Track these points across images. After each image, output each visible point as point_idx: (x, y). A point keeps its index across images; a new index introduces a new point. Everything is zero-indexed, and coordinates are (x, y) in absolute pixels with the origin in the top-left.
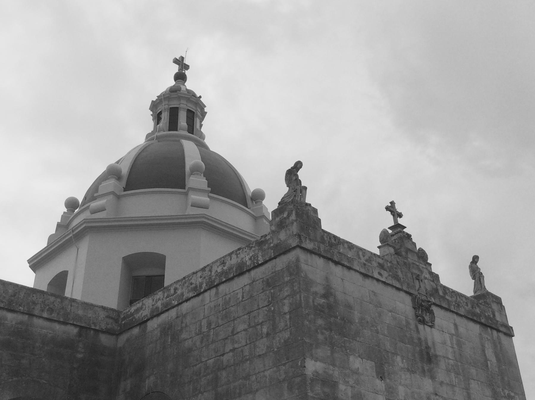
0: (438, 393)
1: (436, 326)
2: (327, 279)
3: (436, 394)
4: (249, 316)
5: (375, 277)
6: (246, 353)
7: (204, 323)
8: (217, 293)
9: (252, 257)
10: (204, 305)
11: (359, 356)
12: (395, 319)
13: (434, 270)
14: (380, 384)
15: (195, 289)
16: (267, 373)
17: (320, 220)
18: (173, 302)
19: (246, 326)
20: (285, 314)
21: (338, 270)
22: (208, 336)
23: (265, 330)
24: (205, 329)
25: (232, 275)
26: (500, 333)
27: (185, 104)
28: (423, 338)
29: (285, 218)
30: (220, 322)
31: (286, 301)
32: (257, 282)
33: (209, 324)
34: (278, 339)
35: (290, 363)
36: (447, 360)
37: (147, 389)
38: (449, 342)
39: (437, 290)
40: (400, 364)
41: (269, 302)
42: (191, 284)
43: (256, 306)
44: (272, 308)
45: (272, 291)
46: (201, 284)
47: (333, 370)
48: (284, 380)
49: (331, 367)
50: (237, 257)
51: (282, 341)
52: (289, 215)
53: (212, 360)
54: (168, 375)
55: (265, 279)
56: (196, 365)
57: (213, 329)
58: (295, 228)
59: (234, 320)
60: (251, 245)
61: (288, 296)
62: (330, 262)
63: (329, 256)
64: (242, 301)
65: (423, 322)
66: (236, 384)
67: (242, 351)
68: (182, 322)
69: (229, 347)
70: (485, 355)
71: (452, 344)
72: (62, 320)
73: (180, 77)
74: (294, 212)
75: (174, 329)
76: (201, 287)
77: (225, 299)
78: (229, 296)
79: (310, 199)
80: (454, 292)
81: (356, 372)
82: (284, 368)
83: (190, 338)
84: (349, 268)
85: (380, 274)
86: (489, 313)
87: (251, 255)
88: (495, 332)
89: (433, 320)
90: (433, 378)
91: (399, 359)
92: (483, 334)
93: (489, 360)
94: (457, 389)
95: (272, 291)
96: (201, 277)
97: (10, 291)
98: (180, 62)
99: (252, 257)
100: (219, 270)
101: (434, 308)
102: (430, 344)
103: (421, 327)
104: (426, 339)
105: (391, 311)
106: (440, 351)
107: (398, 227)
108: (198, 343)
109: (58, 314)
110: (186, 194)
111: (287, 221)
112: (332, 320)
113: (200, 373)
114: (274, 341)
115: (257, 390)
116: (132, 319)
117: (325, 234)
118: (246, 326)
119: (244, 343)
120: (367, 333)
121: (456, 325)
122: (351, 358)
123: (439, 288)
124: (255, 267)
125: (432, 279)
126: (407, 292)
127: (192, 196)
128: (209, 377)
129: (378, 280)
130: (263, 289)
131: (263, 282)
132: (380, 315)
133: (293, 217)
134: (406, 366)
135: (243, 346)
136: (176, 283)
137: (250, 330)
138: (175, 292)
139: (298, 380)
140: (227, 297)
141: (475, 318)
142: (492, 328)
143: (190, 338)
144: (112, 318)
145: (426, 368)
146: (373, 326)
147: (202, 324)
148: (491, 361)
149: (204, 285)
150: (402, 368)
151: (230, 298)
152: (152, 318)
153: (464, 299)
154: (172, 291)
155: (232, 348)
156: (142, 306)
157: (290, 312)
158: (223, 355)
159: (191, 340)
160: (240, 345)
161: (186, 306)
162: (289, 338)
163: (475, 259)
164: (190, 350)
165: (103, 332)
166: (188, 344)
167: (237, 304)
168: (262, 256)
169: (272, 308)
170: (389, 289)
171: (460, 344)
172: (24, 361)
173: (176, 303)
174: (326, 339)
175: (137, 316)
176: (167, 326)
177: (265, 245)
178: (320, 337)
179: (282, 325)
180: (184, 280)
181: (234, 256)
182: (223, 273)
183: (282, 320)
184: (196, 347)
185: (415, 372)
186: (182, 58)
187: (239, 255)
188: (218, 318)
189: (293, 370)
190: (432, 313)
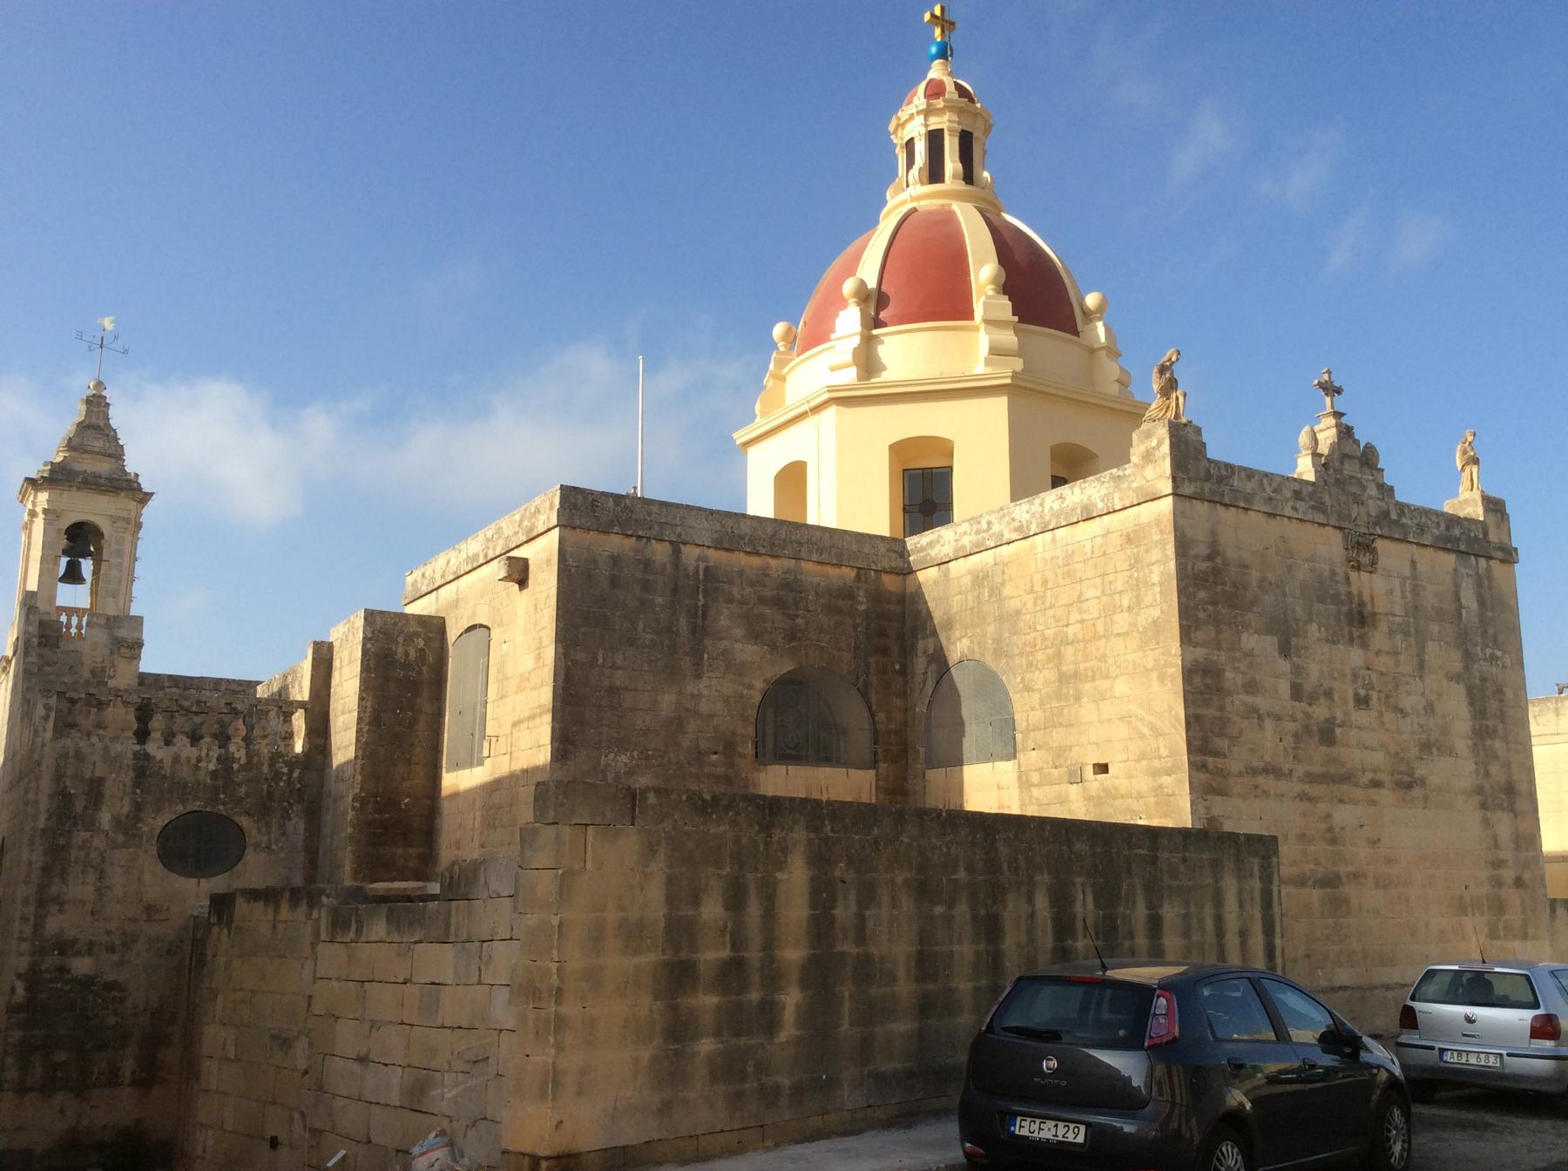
0: (1370, 667)
2: (1213, 533)
3: (1368, 669)
4: (1103, 579)
5: (1287, 514)
6: (1100, 629)
7: (1037, 578)
8: (1054, 540)
9: (1106, 499)
10: (1035, 554)
11: (1255, 633)
12: (1313, 570)
13: (1388, 480)
14: (1284, 666)
15: (1019, 529)
16: (1130, 657)
18: (988, 542)
19: (1099, 594)
20: (1154, 584)
22: (1044, 597)
23: (1125, 602)
24: (1038, 588)
25: (1075, 520)
26: (1493, 561)
28: (1355, 592)
29: (1154, 448)
30: (1061, 582)
31: (1155, 568)
32: (1114, 535)
33: (1045, 582)
34: (1143, 616)
35: (1161, 650)
36: (1391, 619)
37: (959, 654)
38: (1398, 592)
39: (1386, 514)
40: (1317, 634)
41: (1130, 565)
42: (1013, 520)
43: (1113, 568)
44: (1136, 575)
45: (1135, 551)
46: (1029, 523)
47: (1218, 656)
48: (1152, 670)
49: (1216, 652)
50: (1082, 493)
51: (1150, 620)
53: (1053, 630)
54: (990, 641)
55: (1124, 532)
56: (1029, 634)
57: (1051, 589)
59: (1081, 581)
60: (1103, 479)
61: (1158, 561)
62: (1218, 506)
63: (1216, 499)
64: (1092, 558)
66: (1088, 664)
67: (1094, 625)
69: (1075, 617)
70: (1458, 600)
71: (1403, 592)
72: (834, 562)
75: (993, 580)
76: (1029, 523)
77: (1067, 550)
78: (1073, 547)
80: (1417, 509)
81: (1250, 654)
82: (1152, 653)
83: (1019, 596)
85: (1294, 509)
86: (1478, 532)
87: (1103, 493)
88: (1482, 561)
89: (1374, 563)
90: (1364, 645)
91: (1314, 627)
92: (1459, 568)
93: (1465, 608)
94: (1402, 658)
95: (1135, 551)
96: (1028, 512)
97: (769, 530)
99: (1106, 499)
102: (1366, 598)
103: (1353, 575)
104: (1360, 594)
105: (1307, 560)
106: (1381, 606)
108: (1030, 605)
109: (829, 554)
111: (1157, 453)
112: (1219, 589)
113: (1035, 646)
114: (1139, 618)
115: (1117, 677)
116: (926, 556)
117: (1213, 465)
118: (1099, 594)
119: (1096, 615)
120: (1268, 599)
121: (1413, 564)
122: (1244, 636)
123: (1392, 508)
125: (1381, 497)
128: (1050, 651)
130: (1121, 545)
131: (1121, 535)
132: (1290, 568)
134: (1324, 635)
135: (1095, 619)
136: (991, 512)
137: (1105, 598)
140: (1070, 549)
141: (1449, 546)
142: (1477, 556)
143: (1019, 596)
144: (896, 552)
145: (1356, 634)
146: (1278, 587)
147: (1034, 579)
148: (1469, 608)
150: (1318, 640)
151: (1073, 551)
153: (1434, 518)
154: (985, 526)
155: (1079, 619)
156: (938, 538)
157: (1161, 584)
158: (1067, 626)
159: (1019, 598)
160: (1091, 617)
162: (1159, 618)
164: (1018, 612)
165: (885, 571)
166: (1013, 604)
167: (1085, 560)
168: (1120, 499)
169: (1136, 575)
171: (1416, 590)
172: (800, 621)
174: (1210, 616)
175: (933, 553)
176: (981, 574)
177: (1124, 483)
178: (1202, 615)
179: (1148, 599)
180: (1002, 512)
183: (1149, 592)
184: (1027, 609)
185: (1339, 642)
187: (1084, 491)
188: (1056, 574)
189: (1165, 658)
190: (1373, 551)
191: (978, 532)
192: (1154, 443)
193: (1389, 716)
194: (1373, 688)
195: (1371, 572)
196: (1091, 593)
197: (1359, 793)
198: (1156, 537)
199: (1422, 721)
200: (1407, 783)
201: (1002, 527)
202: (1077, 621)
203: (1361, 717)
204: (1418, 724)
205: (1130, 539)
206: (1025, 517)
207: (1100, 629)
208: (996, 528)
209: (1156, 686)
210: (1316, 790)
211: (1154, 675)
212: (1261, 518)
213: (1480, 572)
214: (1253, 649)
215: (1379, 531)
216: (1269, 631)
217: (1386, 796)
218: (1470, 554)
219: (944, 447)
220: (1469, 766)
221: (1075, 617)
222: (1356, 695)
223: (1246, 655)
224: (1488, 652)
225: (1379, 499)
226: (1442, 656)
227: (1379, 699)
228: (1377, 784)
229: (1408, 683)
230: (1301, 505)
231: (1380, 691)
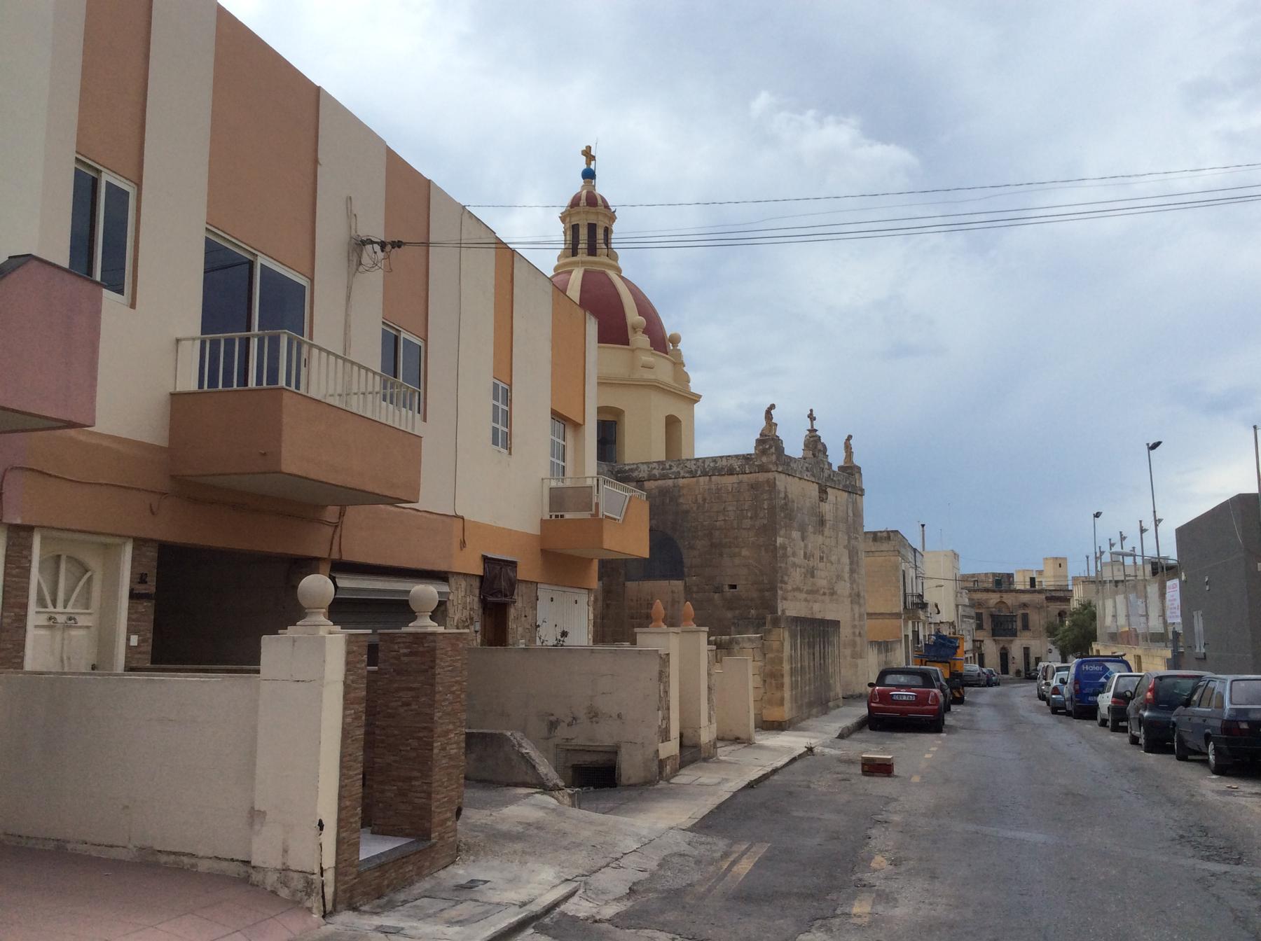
7: (699, 497)
8: (710, 480)
14: (802, 544)
17: (784, 448)
20: (764, 509)
21: (790, 479)
23: (749, 515)
24: (700, 501)
31: (766, 502)
33: (704, 500)
42: (686, 467)
52: (771, 447)
58: (774, 458)
59: (725, 502)
65: (822, 501)
68: (679, 491)
73: (589, 175)
74: (774, 448)
76: (696, 471)
79: (780, 433)
84: (794, 476)
89: (827, 499)
90: (823, 535)
98: (588, 154)
100: (712, 465)
101: (829, 490)
106: (827, 517)
107: (813, 430)
108: (695, 509)
110: (633, 351)
124: (742, 474)
126: (817, 483)
127: (643, 358)
133: (773, 450)
138: (670, 469)
139: (772, 547)
142: (853, 493)
149: (699, 473)
151: (721, 488)
152: (649, 480)
154: (668, 467)
161: (681, 482)
163: (850, 437)
164: (687, 512)
166: (685, 507)
171: (837, 509)
173: (673, 477)
181: (724, 460)
182: (715, 468)
190: (826, 493)
191: (663, 469)
192: (767, 446)
193: (828, 564)
196: (730, 508)
197: (821, 598)
198: (767, 488)
200: (833, 593)
201: (679, 469)
202: (723, 520)
203: (821, 565)
205: (754, 486)
206: (694, 468)
207: (735, 523)
208: (675, 469)
209: (763, 553)
210: (809, 597)
211: (763, 549)
217: (827, 598)
219: (619, 413)
220: (848, 585)
221: (721, 518)
222: (820, 556)
226: (843, 538)
228: (824, 594)
230: (809, 474)
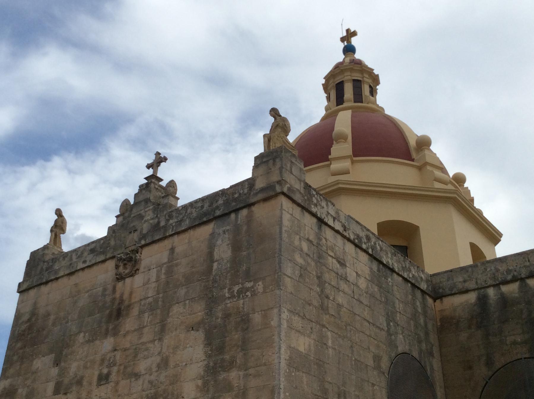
1: (142, 270)
3: (115, 350)
27: (349, 75)
63: (39, 283)
73: (349, 50)
92: (217, 231)
93: (216, 261)
94: (146, 330)
103: (120, 284)
129: (83, 269)
141: (205, 219)
170: (95, 268)
185: (96, 339)
186: (348, 31)
194: (115, 365)
195: (132, 276)
199: (153, 378)
204: (149, 382)
212: (65, 280)
213: (239, 222)
214: (38, 368)
215: (143, 242)
216: (51, 351)
218: (230, 213)
223: (33, 373)
224: (236, 288)
225: (152, 219)
227: (118, 371)
229: (147, 349)
231: (120, 365)
